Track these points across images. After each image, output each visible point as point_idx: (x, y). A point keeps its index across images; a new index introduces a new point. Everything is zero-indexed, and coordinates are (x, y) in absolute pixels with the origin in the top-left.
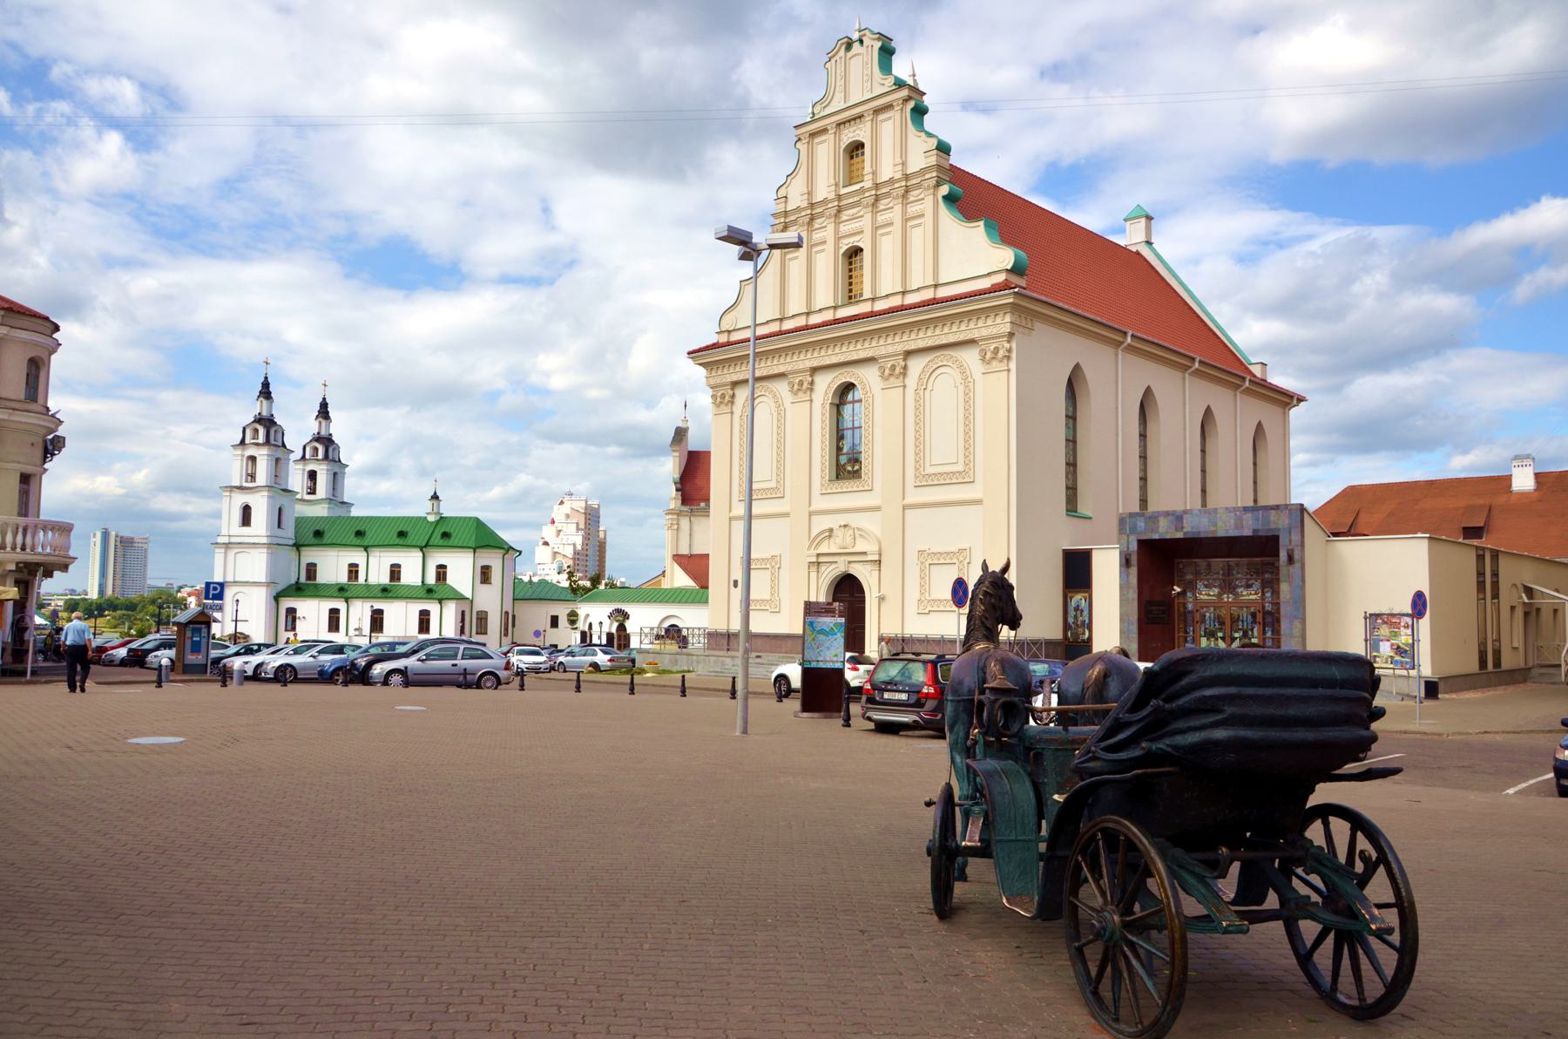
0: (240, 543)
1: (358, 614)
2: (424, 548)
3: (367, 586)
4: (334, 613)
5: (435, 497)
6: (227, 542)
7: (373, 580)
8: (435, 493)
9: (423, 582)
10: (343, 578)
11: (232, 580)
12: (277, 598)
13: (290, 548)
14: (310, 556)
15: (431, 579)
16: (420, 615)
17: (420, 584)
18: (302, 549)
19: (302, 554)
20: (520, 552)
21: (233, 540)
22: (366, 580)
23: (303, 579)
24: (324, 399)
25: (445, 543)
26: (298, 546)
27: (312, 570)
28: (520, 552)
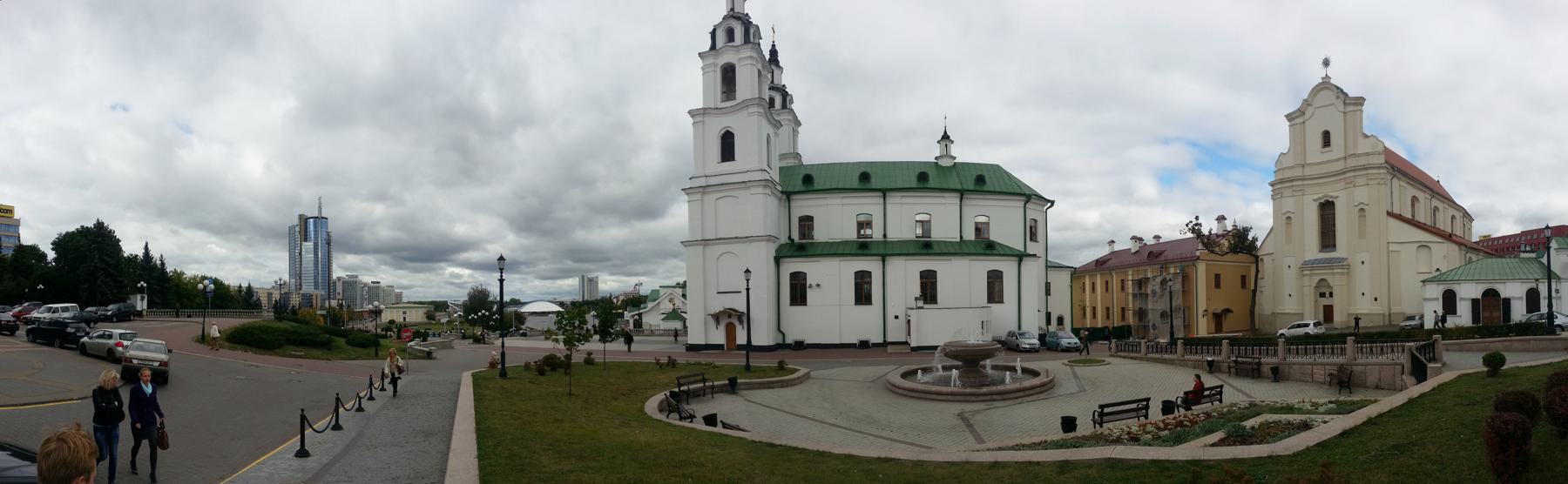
0: (722, 184)
1: (903, 276)
2: (962, 193)
3: (885, 242)
4: (862, 280)
5: (946, 137)
6: (704, 185)
7: (893, 235)
8: (945, 132)
9: (961, 237)
10: (851, 234)
11: (714, 237)
12: (778, 260)
13: (780, 195)
14: (804, 206)
15: (970, 235)
16: (988, 278)
17: (958, 240)
18: (794, 197)
19: (792, 204)
20: (1052, 203)
21: (712, 181)
22: (885, 236)
23: (796, 236)
24: (774, 46)
25: (979, 189)
26: (788, 195)
27: (807, 222)
28: (1052, 203)
